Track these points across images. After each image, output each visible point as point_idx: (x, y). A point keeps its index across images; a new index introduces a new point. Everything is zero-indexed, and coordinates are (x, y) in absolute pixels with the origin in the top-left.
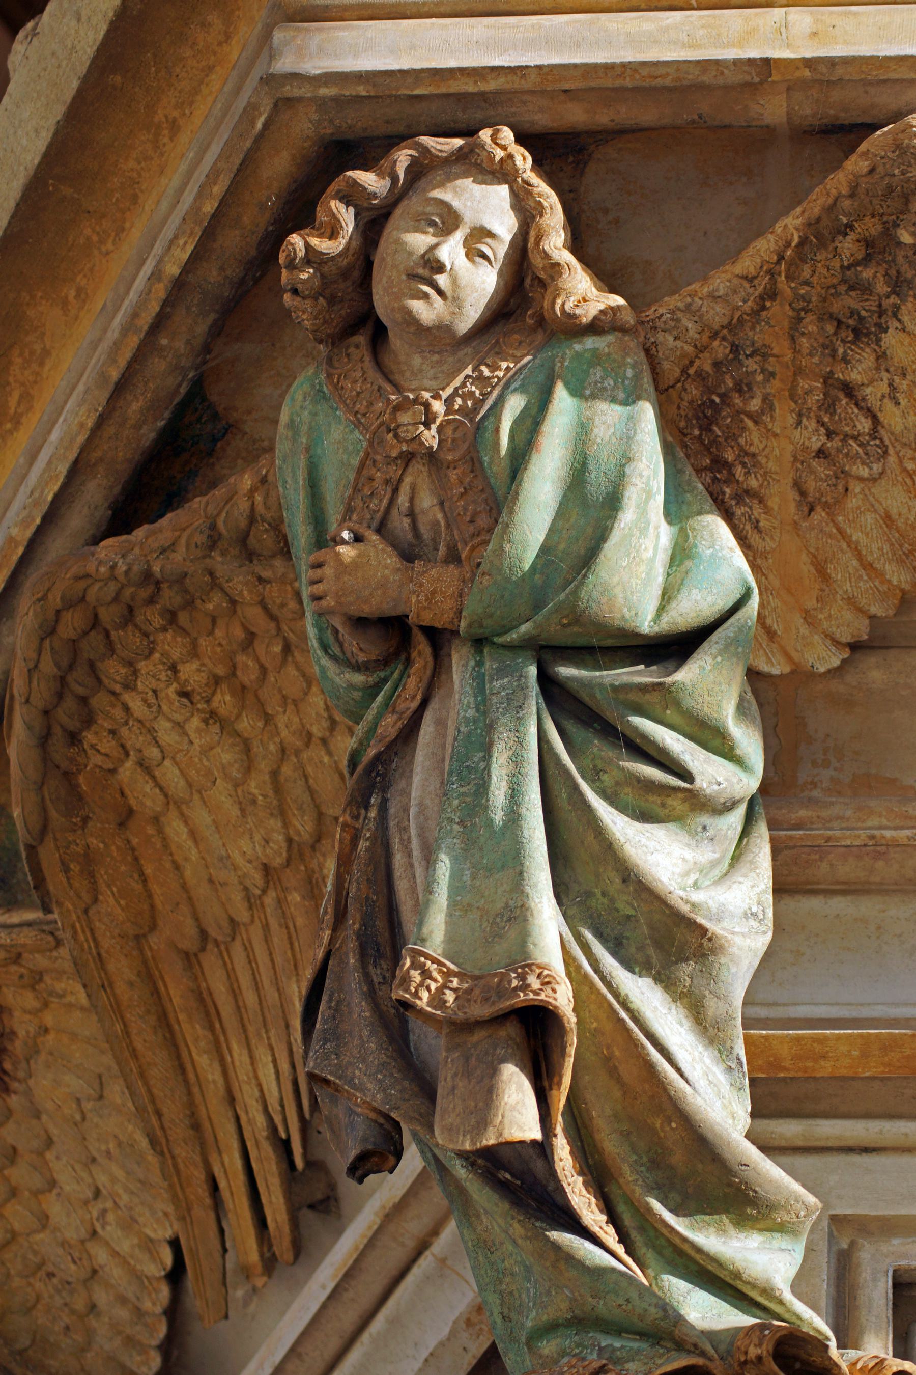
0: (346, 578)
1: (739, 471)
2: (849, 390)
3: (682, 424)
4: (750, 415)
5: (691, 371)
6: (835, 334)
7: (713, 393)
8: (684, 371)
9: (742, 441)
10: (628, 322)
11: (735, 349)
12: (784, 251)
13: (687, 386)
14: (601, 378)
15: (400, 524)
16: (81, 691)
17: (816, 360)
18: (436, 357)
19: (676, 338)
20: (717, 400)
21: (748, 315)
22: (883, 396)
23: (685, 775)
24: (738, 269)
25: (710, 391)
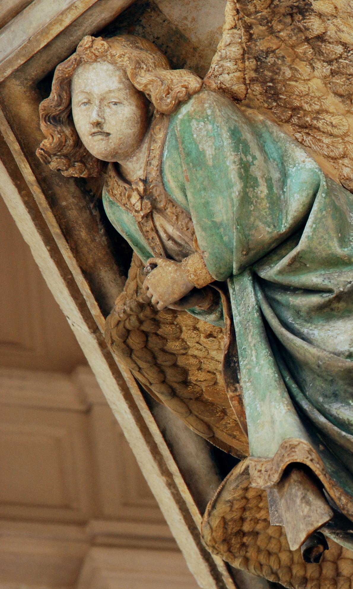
0: (158, 289)
1: (306, 107)
2: (321, 38)
3: (266, 105)
4: (290, 79)
5: (248, 82)
6: (293, 20)
7: (267, 82)
8: (245, 84)
9: (297, 93)
10: (196, 87)
11: (257, 59)
12: (236, 7)
13: (253, 89)
14: (197, 125)
15: (170, 244)
16: (168, 363)
17: (294, 38)
18: (135, 158)
19: (228, 74)
20: (271, 84)
21: (248, 42)
22: (336, 32)
23: (330, 291)
24: (227, 26)
25: (264, 82)
